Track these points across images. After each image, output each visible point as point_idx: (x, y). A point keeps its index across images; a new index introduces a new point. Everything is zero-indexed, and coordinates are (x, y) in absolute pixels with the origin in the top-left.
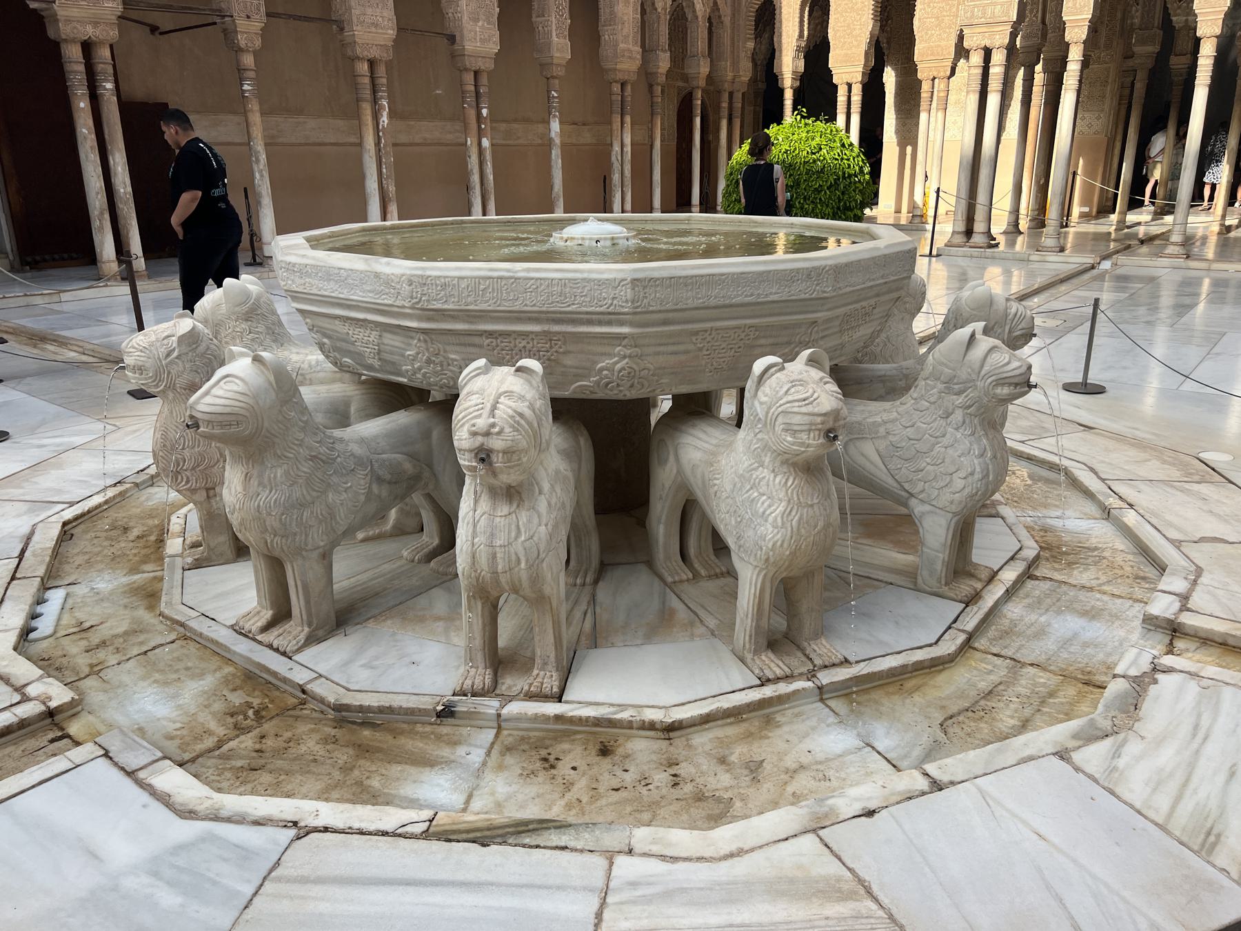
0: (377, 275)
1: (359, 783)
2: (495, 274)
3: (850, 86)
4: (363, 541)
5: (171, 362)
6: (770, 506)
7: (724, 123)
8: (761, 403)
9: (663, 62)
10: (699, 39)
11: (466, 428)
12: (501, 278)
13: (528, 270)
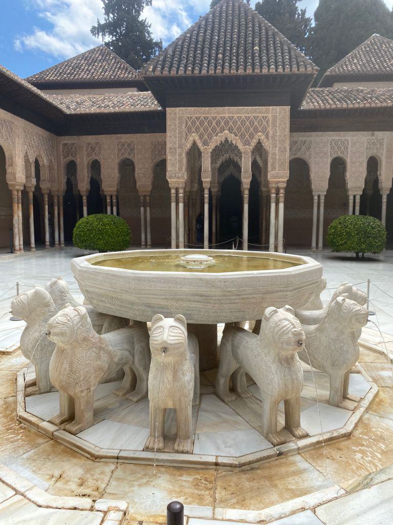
0: (201, 279)
1: (288, 490)
2: (250, 276)
3: (111, 197)
4: (137, 402)
5: (79, 328)
6: (349, 347)
7: (56, 208)
8: (344, 313)
9: (34, 181)
10: (45, 174)
11: (290, 333)
12: (252, 277)
13: (260, 274)
